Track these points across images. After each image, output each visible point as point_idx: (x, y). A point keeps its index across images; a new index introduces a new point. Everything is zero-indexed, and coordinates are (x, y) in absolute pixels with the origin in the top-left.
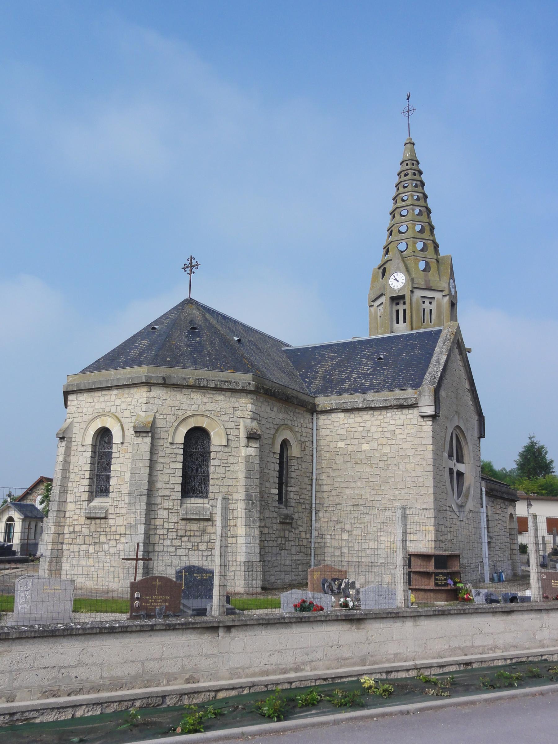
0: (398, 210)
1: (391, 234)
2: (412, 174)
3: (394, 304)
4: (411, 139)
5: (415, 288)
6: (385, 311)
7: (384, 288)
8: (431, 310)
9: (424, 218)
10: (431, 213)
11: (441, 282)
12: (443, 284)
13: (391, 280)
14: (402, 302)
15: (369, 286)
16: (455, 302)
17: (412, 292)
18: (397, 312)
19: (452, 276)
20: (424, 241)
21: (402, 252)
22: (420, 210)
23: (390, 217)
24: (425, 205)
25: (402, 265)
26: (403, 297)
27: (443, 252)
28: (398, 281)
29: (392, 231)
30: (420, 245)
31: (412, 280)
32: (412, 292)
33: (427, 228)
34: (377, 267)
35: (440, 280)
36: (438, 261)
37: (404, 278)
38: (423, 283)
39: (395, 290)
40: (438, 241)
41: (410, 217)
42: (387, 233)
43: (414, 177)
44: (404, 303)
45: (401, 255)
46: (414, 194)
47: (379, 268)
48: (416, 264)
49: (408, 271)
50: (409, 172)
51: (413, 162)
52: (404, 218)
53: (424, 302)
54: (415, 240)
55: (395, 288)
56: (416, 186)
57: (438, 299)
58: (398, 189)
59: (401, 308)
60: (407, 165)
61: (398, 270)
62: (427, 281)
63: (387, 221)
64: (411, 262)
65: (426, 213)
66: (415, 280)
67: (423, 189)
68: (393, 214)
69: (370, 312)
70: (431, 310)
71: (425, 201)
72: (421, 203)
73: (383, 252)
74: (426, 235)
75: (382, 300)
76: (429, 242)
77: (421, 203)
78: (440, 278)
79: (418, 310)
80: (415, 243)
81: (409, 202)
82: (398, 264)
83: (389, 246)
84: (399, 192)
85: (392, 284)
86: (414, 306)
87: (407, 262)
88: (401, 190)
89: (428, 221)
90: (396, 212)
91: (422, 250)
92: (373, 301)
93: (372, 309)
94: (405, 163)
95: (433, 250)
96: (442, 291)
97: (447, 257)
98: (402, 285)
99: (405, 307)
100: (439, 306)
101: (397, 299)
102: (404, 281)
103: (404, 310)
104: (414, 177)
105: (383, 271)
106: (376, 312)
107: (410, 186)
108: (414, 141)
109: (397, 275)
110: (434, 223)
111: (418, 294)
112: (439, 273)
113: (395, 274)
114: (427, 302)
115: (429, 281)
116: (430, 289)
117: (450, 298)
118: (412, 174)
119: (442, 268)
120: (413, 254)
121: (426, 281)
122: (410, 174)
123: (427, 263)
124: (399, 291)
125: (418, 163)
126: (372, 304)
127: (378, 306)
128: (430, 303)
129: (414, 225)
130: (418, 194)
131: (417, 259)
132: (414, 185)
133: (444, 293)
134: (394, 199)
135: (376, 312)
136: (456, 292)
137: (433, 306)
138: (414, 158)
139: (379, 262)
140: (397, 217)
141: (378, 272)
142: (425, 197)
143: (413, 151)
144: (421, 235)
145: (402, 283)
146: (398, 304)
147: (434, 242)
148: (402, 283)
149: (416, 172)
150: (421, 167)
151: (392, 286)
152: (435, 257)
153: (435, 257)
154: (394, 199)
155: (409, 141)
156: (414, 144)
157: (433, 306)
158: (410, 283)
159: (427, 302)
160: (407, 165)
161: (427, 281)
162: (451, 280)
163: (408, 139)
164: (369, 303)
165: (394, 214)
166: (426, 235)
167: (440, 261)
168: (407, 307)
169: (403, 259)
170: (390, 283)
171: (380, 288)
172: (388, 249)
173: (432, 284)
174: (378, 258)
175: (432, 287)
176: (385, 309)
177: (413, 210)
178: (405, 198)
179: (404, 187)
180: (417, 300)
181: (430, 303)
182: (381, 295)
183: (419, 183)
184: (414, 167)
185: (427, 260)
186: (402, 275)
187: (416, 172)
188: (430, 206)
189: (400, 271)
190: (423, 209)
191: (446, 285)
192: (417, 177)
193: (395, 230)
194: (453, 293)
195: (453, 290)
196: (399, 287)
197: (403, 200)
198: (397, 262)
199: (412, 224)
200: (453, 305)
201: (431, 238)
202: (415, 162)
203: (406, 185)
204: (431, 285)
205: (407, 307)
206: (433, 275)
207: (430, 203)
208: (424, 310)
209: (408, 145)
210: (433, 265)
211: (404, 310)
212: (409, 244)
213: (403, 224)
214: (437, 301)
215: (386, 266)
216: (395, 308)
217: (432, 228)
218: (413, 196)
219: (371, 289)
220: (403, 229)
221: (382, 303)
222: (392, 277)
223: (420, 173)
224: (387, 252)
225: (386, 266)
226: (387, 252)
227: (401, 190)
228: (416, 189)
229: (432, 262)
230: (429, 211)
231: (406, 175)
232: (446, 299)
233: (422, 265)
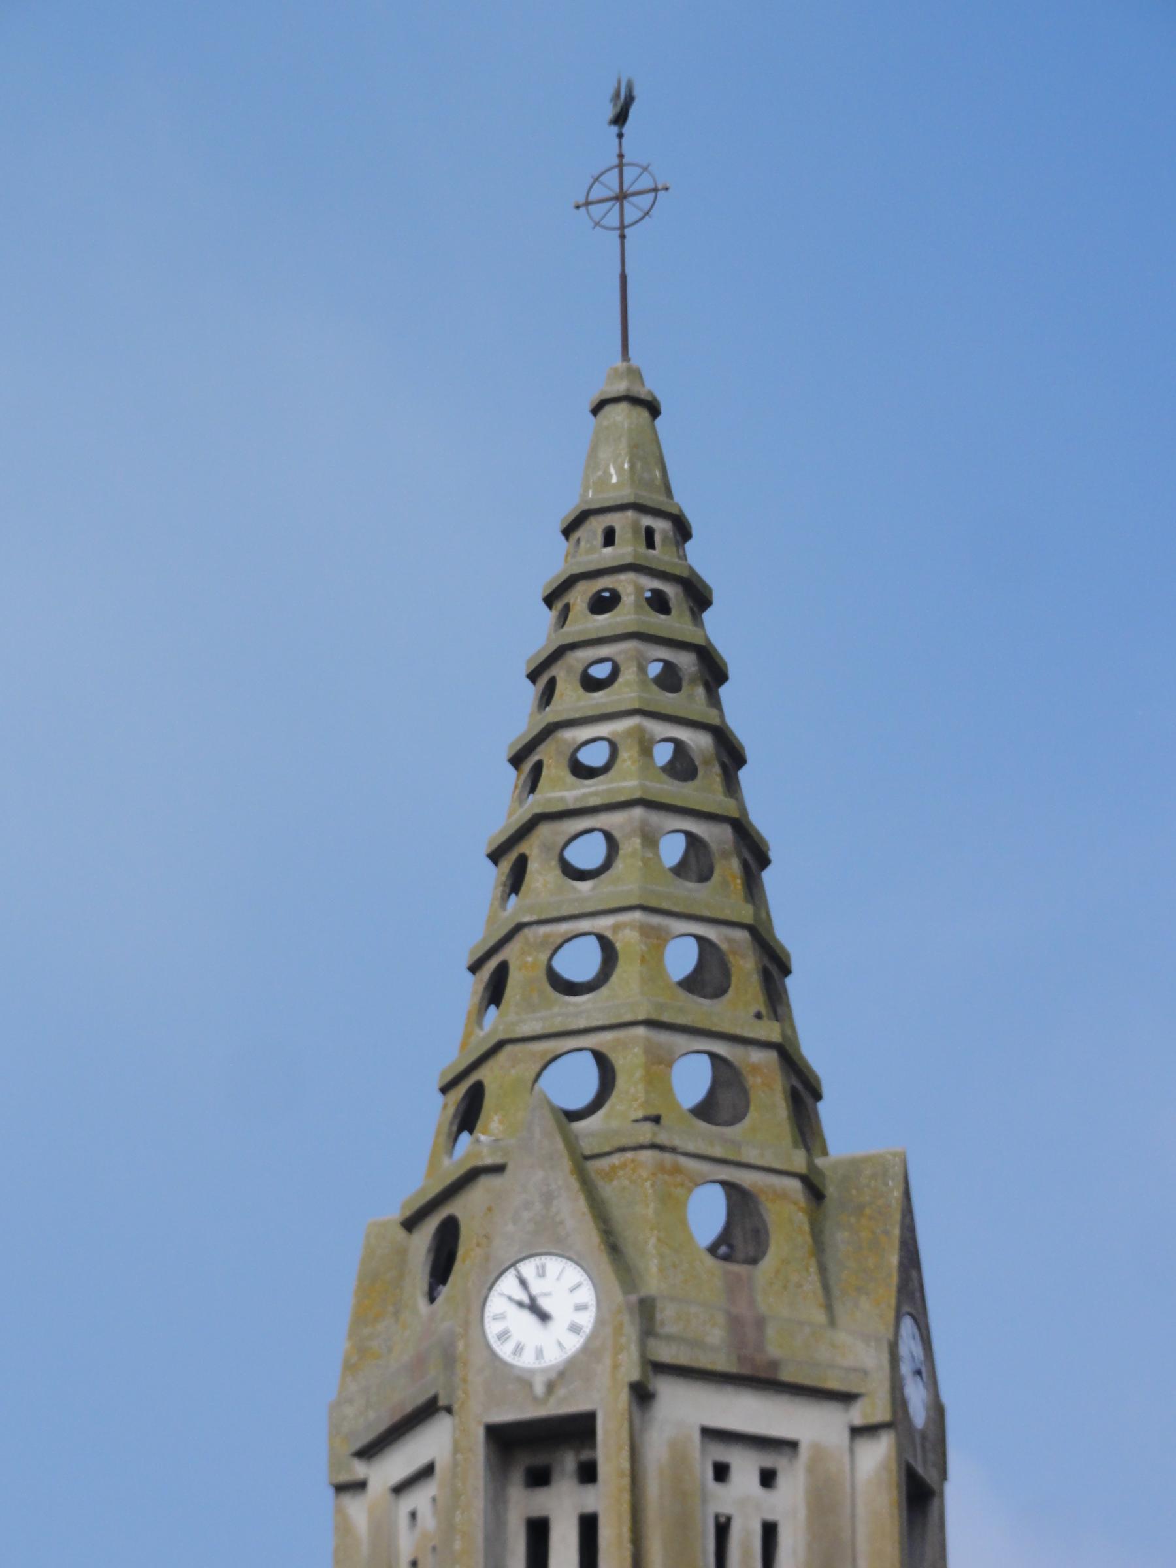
0: (545, 830)
1: (495, 992)
2: (639, 596)
3: (517, 1476)
4: (635, 374)
5: (660, 1368)
6: (448, 1528)
7: (450, 1359)
8: (770, 1531)
9: (722, 893)
10: (786, 971)
11: (841, 1337)
12: (855, 1348)
13: (497, 1304)
14: (569, 1462)
15: (339, 1345)
16: (928, 1474)
17: (642, 1395)
18: (538, 1531)
19: (911, 1295)
20: (721, 1048)
21: (574, 1116)
22: (689, 835)
23: (493, 876)
24: (728, 807)
25: (571, 1209)
26: (579, 1430)
27: (849, 1128)
28: (543, 1319)
29: (502, 971)
30: (692, 1079)
31: (646, 1310)
32: (642, 1395)
33: (745, 966)
34: (395, 1212)
35: (832, 1322)
36: (814, 1190)
37: (587, 1294)
38: (716, 1335)
39: (523, 1380)
40: (812, 1052)
41: (628, 880)
42: (471, 987)
43: (657, 623)
44: (588, 1474)
45: (571, 1143)
46: (660, 729)
47: (411, 1224)
48: (673, 1205)
49: (614, 1249)
50: (626, 584)
51: (647, 521)
52: (585, 886)
53: (721, 1472)
54: (664, 1037)
55: (527, 1361)
56: (670, 679)
57: (819, 1453)
58: (547, 696)
59: (563, 1505)
60: (609, 538)
61: (548, 1240)
62: (744, 1328)
63: (471, 904)
64: (632, 1189)
65: (735, 864)
66: (667, 1313)
67: (714, 700)
68: (510, 857)
69: (343, 1527)
70: (770, 1531)
71: (731, 785)
72: (705, 791)
73: (437, 1110)
74: (738, 1009)
75: (432, 1443)
76: (757, 1056)
77: (705, 791)
78: (829, 1307)
79: (682, 1524)
80: (659, 1064)
81: (626, 780)
82: (548, 1198)
83: (484, 1074)
84: (553, 714)
85: (504, 1336)
86: (653, 1489)
87: (608, 1190)
88: (571, 699)
89: (746, 913)
90: (532, 847)
91: (706, 1111)
92: (370, 1451)
93: (357, 1509)
94: (597, 525)
95: (782, 1110)
96: (846, 1398)
97: (878, 1166)
98: (574, 1343)
99: (591, 1499)
100: (825, 1503)
101: (540, 1445)
102: (587, 1320)
103: (588, 1526)
104: (657, 623)
105: (444, 1248)
106: (383, 1532)
107: (628, 674)
108: (654, 385)
109: (542, 1273)
110: (785, 933)
111: (685, 1409)
112: (823, 1270)
113: (528, 1269)
114: (745, 1466)
115: (760, 1323)
116: (762, 1380)
117: (900, 1449)
118: (639, 596)
119: (840, 1238)
120: (646, 1133)
121: (735, 1323)
122: (628, 599)
123: (740, 1200)
124: (551, 1387)
125: (682, 530)
126: (360, 1470)
127: (400, 1489)
128: (768, 1478)
129: (657, 940)
130: (683, 734)
131: (677, 1170)
132: (655, 669)
133: (857, 1415)
134: (516, 761)
135: (383, 1532)
136: (938, 1411)
137: (788, 1503)
138: (655, 499)
139: (413, 1182)
140: (542, 877)
141: (402, 1253)
142: (731, 756)
143: (649, 456)
144: (698, 1010)
145: (575, 1329)
146: (539, 1478)
147: (742, 830)
148: (575, 1329)
149: (671, 591)
150: (700, 556)
151: (505, 1351)
152: (798, 1161)
153: (798, 1161)
154: (516, 761)
155: (621, 387)
156: (653, 409)
157: (788, 1503)
158: (631, 1331)
159: (745, 1466)
160: (609, 538)
161: (744, 1328)
162: (907, 1325)
163: (616, 374)
164: (335, 1464)
165: (522, 861)
166: (738, 1009)
167: (831, 1191)
168: (606, 1499)
169: (581, 1161)
170: (492, 1329)
171: (418, 1364)
172: (476, 1097)
173: (779, 1348)
174: (407, 1155)
175: (774, 1365)
176: (446, 1510)
177: (650, 840)
178: (594, 756)
179: (591, 684)
180: (678, 1459)
181: (768, 1478)
182: (427, 1411)
183: (686, 661)
184: (661, 556)
185: (746, 1178)
186: (573, 1274)
187: (671, 591)
188: (761, 820)
189: (560, 1248)
190: (716, 835)
191: (873, 1359)
192: (676, 624)
193: (523, 962)
194: (919, 1415)
195: (916, 1395)
196: (554, 1357)
197: (582, 771)
198: (539, 1180)
199: (645, 931)
200: (919, 1496)
201: (770, 1031)
202: (661, 526)
203: (601, 671)
204: (774, 1350)
205: (606, 1499)
206: (780, 1279)
207: (763, 797)
208: (723, 1529)
209: (619, 414)
210: (785, 1211)
211: (588, 1526)
212: (620, 1061)
213: (585, 925)
214: (811, 1470)
215: (464, 1208)
216: (523, 1503)
217: (775, 965)
218: (646, 748)
219: (350, 1368)
220: (579, 962)
221: (428, 1471)
222: (508, 1284)
223: (699, 597)
224: (468, 1116)
225: (464, 1208)
226: (468, 1116)
227: (571, 699)
228: (668, 701)
229: (783, 1196)
230: (754, 854)
231: (603, 603)
232: (876, 1456)
233: (707, 1213)
